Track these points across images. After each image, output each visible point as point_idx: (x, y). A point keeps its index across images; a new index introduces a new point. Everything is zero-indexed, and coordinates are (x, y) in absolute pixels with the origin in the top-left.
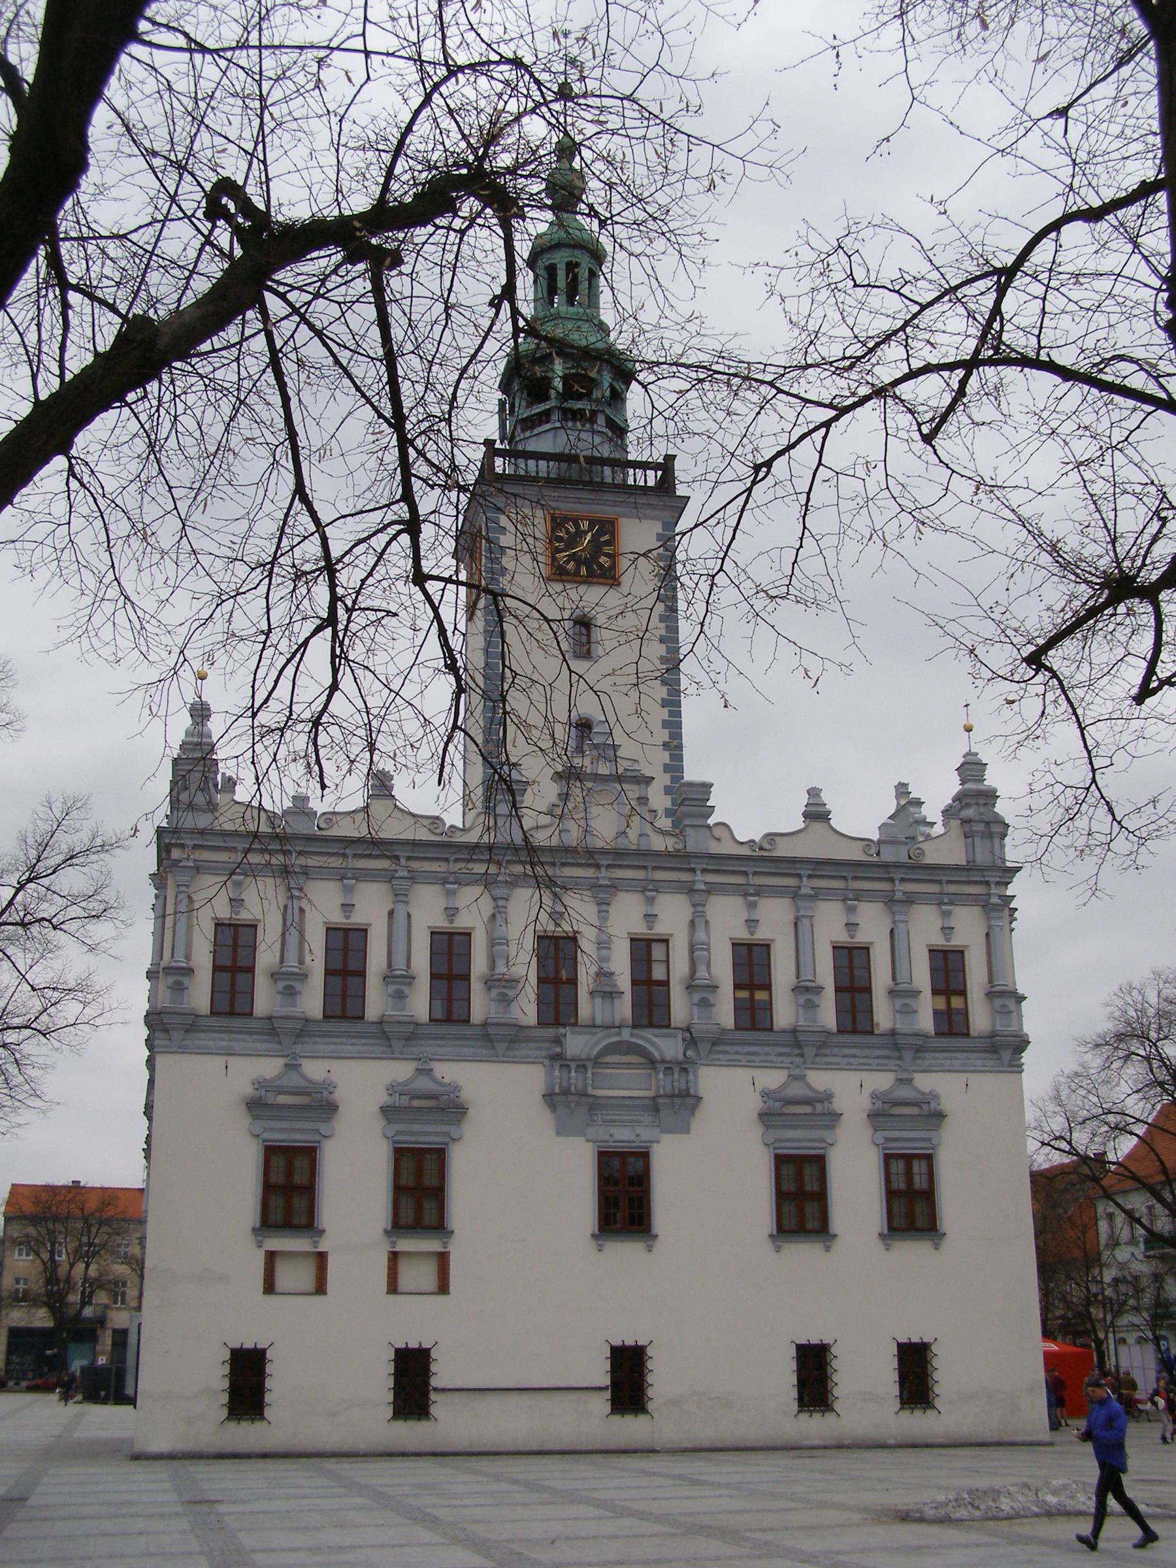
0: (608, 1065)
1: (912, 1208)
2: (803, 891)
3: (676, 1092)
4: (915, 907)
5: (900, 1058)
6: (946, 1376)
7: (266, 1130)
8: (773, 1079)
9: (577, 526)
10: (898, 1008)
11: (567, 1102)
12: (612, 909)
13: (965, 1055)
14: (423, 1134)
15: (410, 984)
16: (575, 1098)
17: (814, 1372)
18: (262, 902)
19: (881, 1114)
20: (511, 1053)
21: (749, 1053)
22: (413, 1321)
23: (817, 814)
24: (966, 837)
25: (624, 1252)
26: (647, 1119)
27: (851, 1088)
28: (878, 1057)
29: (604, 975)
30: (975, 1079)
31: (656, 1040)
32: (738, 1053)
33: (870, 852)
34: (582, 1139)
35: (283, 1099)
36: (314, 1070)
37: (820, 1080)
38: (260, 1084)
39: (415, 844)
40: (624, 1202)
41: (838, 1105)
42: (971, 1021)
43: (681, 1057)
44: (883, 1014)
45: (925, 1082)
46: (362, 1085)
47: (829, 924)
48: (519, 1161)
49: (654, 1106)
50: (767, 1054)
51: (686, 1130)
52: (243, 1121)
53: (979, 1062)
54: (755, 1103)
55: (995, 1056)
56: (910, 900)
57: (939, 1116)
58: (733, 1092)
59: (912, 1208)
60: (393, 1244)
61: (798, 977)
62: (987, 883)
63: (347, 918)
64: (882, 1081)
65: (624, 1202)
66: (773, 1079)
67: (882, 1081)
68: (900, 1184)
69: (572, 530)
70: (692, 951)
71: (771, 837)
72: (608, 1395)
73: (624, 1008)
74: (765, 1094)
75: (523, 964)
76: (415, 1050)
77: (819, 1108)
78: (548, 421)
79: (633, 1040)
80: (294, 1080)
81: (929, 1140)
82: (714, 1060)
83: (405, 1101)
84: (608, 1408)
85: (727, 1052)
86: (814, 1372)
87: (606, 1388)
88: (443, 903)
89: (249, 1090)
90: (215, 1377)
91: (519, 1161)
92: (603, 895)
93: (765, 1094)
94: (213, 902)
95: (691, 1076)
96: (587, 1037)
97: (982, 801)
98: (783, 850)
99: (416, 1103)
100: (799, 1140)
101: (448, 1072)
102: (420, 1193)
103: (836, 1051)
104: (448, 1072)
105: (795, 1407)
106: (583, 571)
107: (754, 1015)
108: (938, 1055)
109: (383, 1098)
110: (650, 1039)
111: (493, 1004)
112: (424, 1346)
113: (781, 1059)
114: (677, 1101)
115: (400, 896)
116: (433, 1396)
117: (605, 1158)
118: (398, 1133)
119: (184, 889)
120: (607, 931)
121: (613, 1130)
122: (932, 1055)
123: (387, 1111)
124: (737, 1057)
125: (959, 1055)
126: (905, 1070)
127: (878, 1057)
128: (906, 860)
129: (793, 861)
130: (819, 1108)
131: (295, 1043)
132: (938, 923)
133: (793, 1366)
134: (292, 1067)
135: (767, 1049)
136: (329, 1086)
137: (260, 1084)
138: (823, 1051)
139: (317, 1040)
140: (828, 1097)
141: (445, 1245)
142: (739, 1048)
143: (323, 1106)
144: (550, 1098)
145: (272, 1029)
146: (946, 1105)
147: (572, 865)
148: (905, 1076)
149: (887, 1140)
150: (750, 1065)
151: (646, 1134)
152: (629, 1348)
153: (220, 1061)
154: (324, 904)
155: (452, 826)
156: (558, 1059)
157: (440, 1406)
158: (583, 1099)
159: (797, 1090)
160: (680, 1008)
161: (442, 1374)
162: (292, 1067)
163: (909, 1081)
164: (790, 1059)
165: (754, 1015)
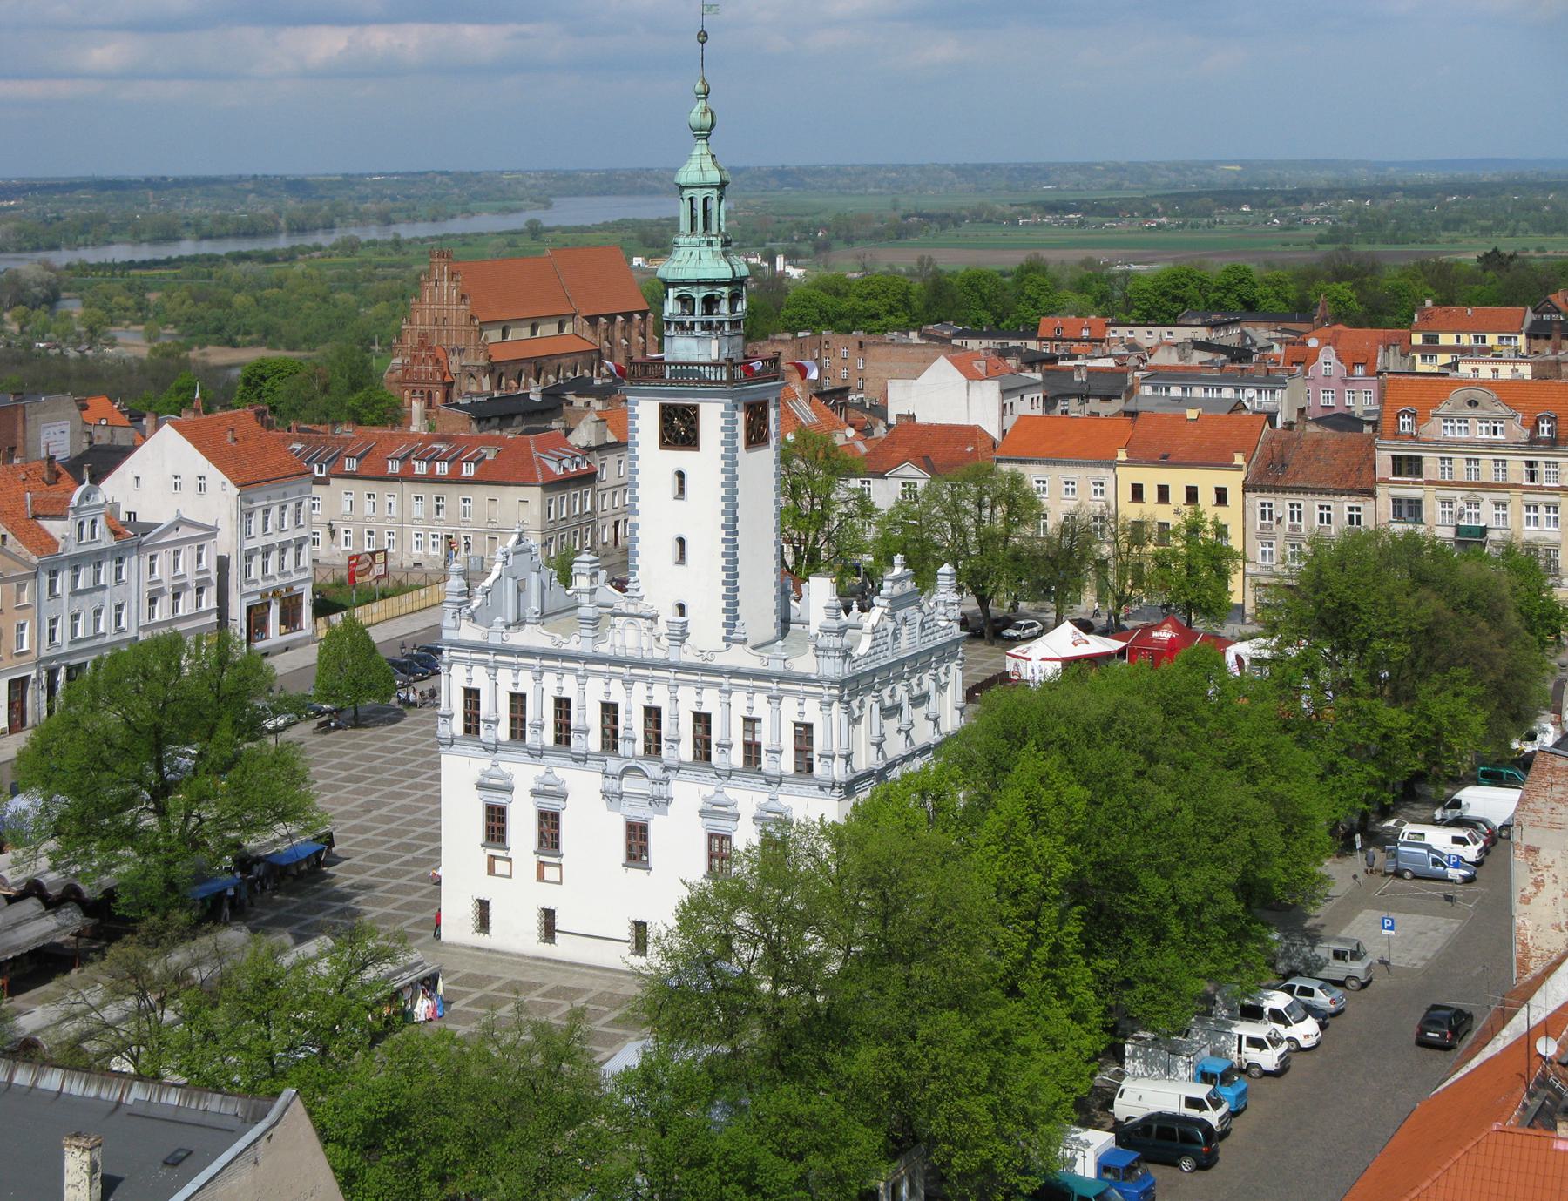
8: (709, 791)
14: (549, 804)
22: (548, 896)
35: (493, 781)
36: (504, 767)
37: (731, 793)
41: (739, 809)
44: (766, 763)
47: (739, 701)
54: (700, 805)
64: (763, 798)
66: (709, 791)
67: (763, 798)
73: (640, 747)
74: (705, 799)
75: (594, 719)
89: (477, 777)
90: (469, 912)
92: (628, 683)
102: (549, 829)
109: (533, 785)
110: (645, 765)
156: (605, 775)
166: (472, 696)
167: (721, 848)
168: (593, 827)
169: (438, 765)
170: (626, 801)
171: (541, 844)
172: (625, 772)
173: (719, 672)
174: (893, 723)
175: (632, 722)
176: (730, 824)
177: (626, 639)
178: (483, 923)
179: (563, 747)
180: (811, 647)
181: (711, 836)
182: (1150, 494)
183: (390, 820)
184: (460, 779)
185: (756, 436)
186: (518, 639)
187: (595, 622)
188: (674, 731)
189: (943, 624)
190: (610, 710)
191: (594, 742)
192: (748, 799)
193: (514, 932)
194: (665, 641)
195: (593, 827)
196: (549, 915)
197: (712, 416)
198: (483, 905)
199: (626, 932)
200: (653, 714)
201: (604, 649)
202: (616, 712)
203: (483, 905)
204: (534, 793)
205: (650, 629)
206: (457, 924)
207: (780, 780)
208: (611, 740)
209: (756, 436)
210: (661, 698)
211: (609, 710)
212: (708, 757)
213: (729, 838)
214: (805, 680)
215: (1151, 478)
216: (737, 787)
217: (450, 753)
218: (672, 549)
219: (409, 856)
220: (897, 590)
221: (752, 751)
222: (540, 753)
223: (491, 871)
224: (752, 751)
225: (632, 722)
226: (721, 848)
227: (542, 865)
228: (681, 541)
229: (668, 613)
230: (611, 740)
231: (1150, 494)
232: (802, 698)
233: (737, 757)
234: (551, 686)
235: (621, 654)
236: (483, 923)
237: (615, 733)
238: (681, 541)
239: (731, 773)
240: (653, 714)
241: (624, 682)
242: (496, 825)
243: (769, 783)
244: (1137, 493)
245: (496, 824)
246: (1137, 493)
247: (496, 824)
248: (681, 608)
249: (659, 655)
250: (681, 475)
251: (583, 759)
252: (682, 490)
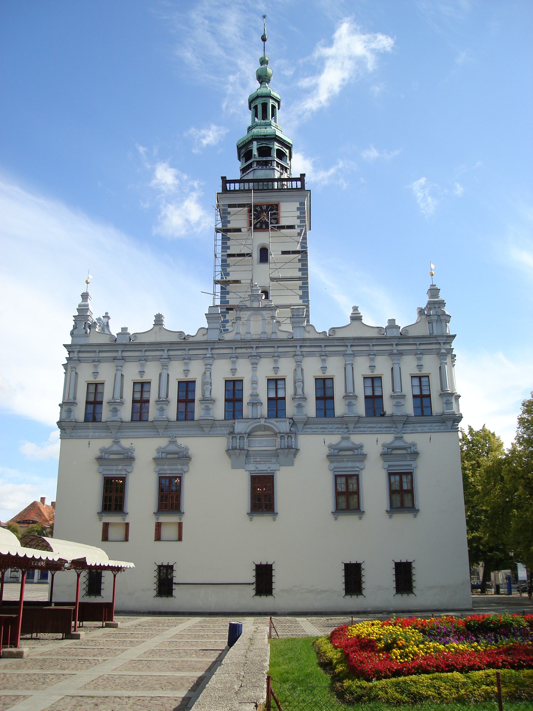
0: (256, 436)
1: (402, 497)
2: (348, 352)
3: (286, 447)
4: (403, 357)
5: (396, 427)
6: (419, 577)
7: (104, 470)
8: (334, 439)
9: (261, 208)
10: (394, 404)
11: (237, 452)
12: (258, 366)
13: (429, 424)
15: (167, 405)
16: (239, 451)
17: (353, 578)
18: (106, 373)
19: (387, 454)
20: (211, 433)
21: (322, 428)
22: (166, 553)
23: (356, 318)
24: (429, 323)
25: (263, 521)
26: (274, 460)
27: (372, 443)
28: (386, 427)
29: (254, 396)
30: (434, 435)
31: (276, 423)
32: (316, 428)
33: (382, 333)
34: (244, 470)
35: (112, 457)
36: (126, 443)
37: (356, 439)
39: (172, 343)
40: (263, 498)
41: (365, 450)
42: (434, 408)
43: (288, 431)
44: (388, 407)
45: (409, 438)
46: (146, 449)
47: (362, 367)
48: (215, 481)
49: (276, 454)
50: (331, 428)
51: (292, 464)
52: (95, 466)
53: (437, 428)
54: (326, 451)
55: (444, 424)
56: (401, 354)
57: (416, 454)
58: (314, 447)
59: (402, 497)
60: (157, 519)
61: (346, 392)
62: (439, 343)
63: (142, 377)
64: (388, 438)
65: (263, 498)
66: (334, 439)
67: (388, 438)
68: (396, 487)
69: (259, 210)
70: (295, 383)
71: (333, 330)
72: (254, 586)
73: (264, 410)
75: (219, 392)
76: (169, 433)
77: (356, 452)
78: (252, 167)
79: (265, 424)
81: (410, 465)
82: (306, 432)
83: (164, 455)
84: (254, 592)
85: (311, 428)
86: (353, 578)
87: (253, 584)
88: (184, 368)
89: (98, 454)
91: (215, 481)
92: (255, 359)
93: (330, 447)
94: (86, 373)
95: (293, 440)
96: (245, 424)
97: (437, 306)
98: (339, 334)
99: (169, 456)
101: (182, 442)
103: (364, 425)
104: (182, 442)
105: (344, 592)
106: (264, 226)
108: (415, 425)
111: (203, 411)
112: (170, 564)
113: (337, 430)
114: (286, 451)
115: (165, 366)
116: (174, 587)
118: (160, 470)
119: (74, 369)
120: (255, 377)
121: (258, 466)
122: (412, 425)
123: (156, 460)
124: (316, 430)
125: (426, 425)
126: (398, 433)
127: (386, 427)
128: (400, 335)
129: (342, 339)
130: (356, 452)
131: (118, 432)
132: (415, 363)
133: (343, 573)
134: (116, 442)
135: (330, 426)
136: (132, 450)
137: (103, 450)
138: (359, 425)
139: (128, 430)
140: (361, 447)
141: (180, 519)
142: (317, 426)
143: (128, 458)
145: (107, 427)
146: (420, 448)
147: (241, 348)
148: (399, 435)
149: (389, 466)
150: (323, 433)
151: (273, 467)
152: (264, 565)
153: (87, 441)
154: (132, 373)
155: (188, 335)
157: (177, 591)
158: (242, 451)
159: (345, 444)
160: (290, 409)
161: (178, 576)
162: (116, 442)
164: (342, 430)
176: (357, 464)
191: (219, 410)
199: (250, 576)
207: (406, 421)
232: (419, 354)
251: (208, 427)
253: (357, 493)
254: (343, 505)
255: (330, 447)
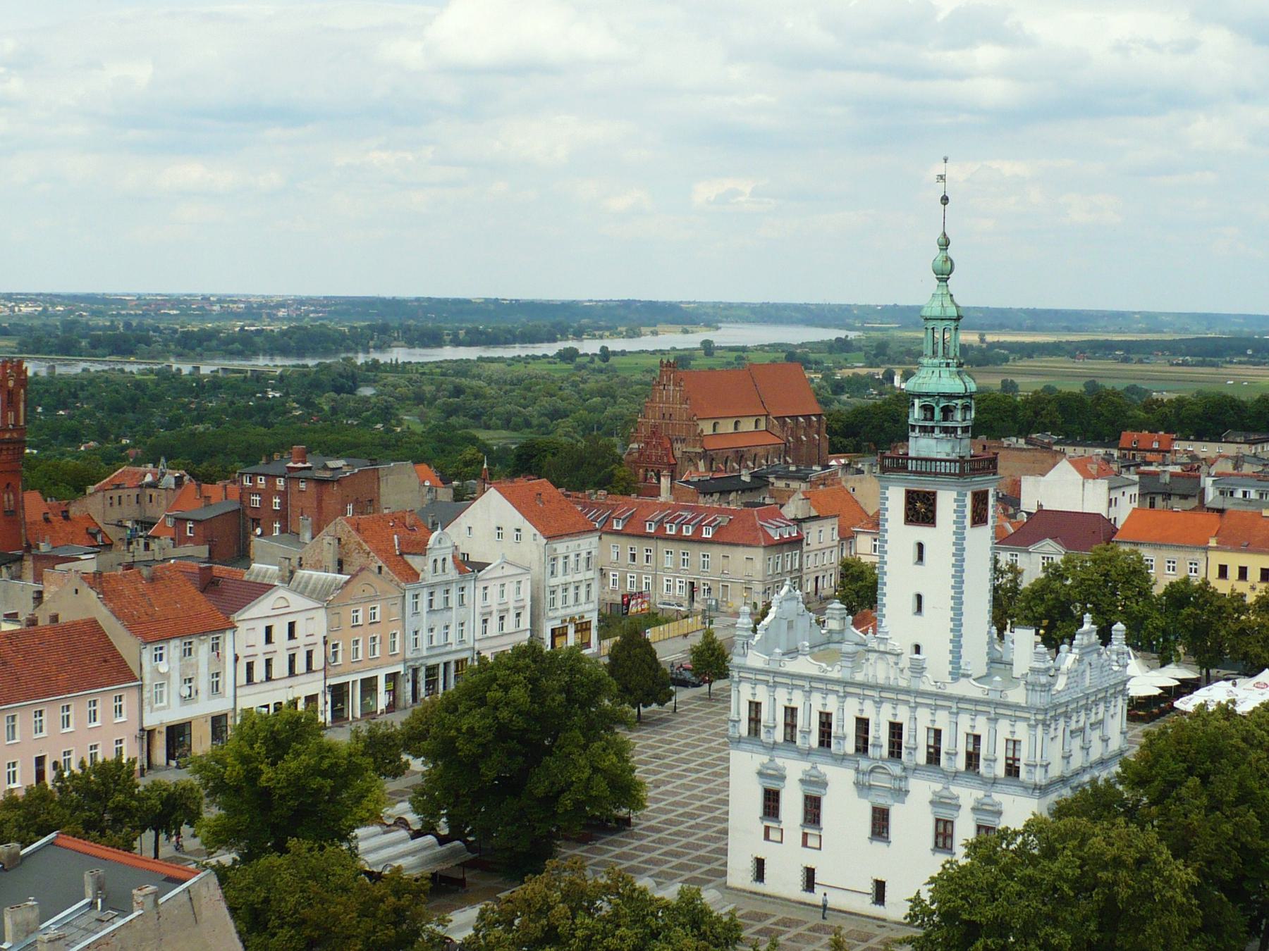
8: (938, 787)
14: (814, 792)
25: (879, 846)
37: (955, 790)
38: (763, 765)
41: (961, 802)
45: (997, 797)
47: (965, 722)
52: (756, 777)
54: (930, 797)
58: (922, 789)
66: (938, 787)
67: (980, 794)
73: (885, 751)
75: (850, 729)
80: (772, 765)
90: (750, 866)
92: (879, 703)
93: (934, 793)
100: (945, 814)
101: (823, 768)
104: (823, 768)
107: (934, 757)
109: (801, 776)
117: (875, 809)
140: (957, 798)
144: (857, 784)
146: (1004, 808)
151: (889, 802)
156: (857, 770)
161: (818, 878)
163: (990, 796)
165: (934, 757)
166: (755, 707)
167: (945, 829)
168: (846, 809)
169: (727, 760)
170: (873, 792)
171: (805, 819)
172: (872, 771)
173: (949, 698)
174: (1077, 742)
175: (880, 734)
177: (877, 671)
178: (760, 875)
179: (826, 749)
180: (1023, 683)
181: (938, 820)
182: (1233, 573)
183: (675, 794)
184: (745, 770)
185: (979, 518)
186: (791, 666)
187: (852, 656)
188: (912, 741)
189: (1116, 668)
190: (863, 724)
191: (850, 746)
192: (968, 795)
193: (784, 881)
194: (907, 673)
195: (846, 809)
196: (810, 874)
197: (947, 502)
198: (760, 863)
199: (869, 888)
200: (896, 730)
201: (859, 677)
202: (867, 724)
203: (760, 863)
204: (802, 781)
205: (896, 664)
206: (739, 873)
207: (995, 781)
208: (863, 746)
209: (979, 518)
210: (903, 716)
211: (863, 724)
212: (938, 761)
213: (952, 822)
214: (1017, 707)
215: (1234, 561)
216: (961, 785)
217: (738, 749)
218: (912, 603)
219: (692, 822)
220: (1085, 642)
221: (972, 759)
222: (808, 753)
223: (767, 837)
224: (972, 759)
225: (880, 734)
226: (945, 829)
227: (805, 835)
228: (919, 597)
229: (908, 653)
230: (863, 746)
231: (1233, 573)
233: (961, 763)
234: (817, 702)
235: (872, 681)
236: (760, 875)
237: (866, 740)
238: (919, 597)
239: (956, 774)
240: (896, 730)
241: (875, 702)
242: (772, 804)
243: (985, 783)
244: (1223, 571)
245: (771, 803)
246: (1223, 571)
247: (771, 803)
248: (917, 649)
249: (903, 683)
250: (920, 546)
252: (920, 558)
253: (951, 836)
254: (941, 845)
255: (934, 793)
